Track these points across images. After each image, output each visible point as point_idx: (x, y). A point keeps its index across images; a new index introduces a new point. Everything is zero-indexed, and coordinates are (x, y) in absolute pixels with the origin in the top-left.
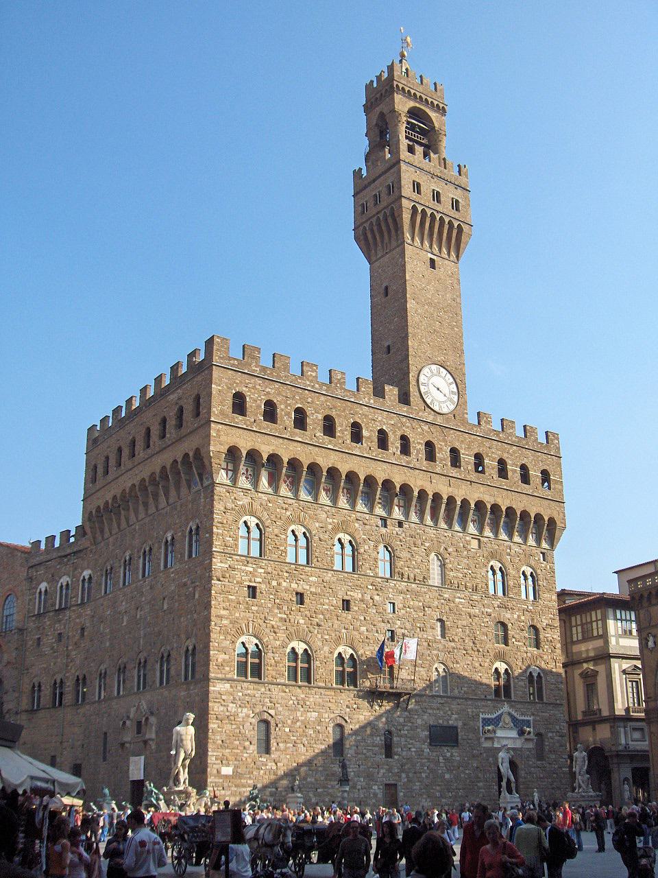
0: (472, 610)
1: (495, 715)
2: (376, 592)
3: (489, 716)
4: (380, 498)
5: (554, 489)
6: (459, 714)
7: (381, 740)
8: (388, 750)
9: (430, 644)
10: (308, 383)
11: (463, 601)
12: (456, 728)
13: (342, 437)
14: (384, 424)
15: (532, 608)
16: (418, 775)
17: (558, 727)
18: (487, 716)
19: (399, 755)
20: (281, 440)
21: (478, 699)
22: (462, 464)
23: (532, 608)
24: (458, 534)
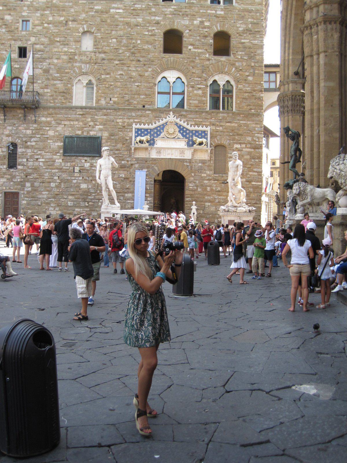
0: (133, 20)
1: (154, 126)
3: (146, 127)
6: (105, 125)
7: (3, 152)
8: (12, 160)
9: (71, 56)
11: (121, 11)
12: (98, 138)
15: (222, 13)
16: (47, 185)
17: (249, 139)
18: (142, 126)
19: (23, 165)
21: (133, 110)
23: (222, 13)
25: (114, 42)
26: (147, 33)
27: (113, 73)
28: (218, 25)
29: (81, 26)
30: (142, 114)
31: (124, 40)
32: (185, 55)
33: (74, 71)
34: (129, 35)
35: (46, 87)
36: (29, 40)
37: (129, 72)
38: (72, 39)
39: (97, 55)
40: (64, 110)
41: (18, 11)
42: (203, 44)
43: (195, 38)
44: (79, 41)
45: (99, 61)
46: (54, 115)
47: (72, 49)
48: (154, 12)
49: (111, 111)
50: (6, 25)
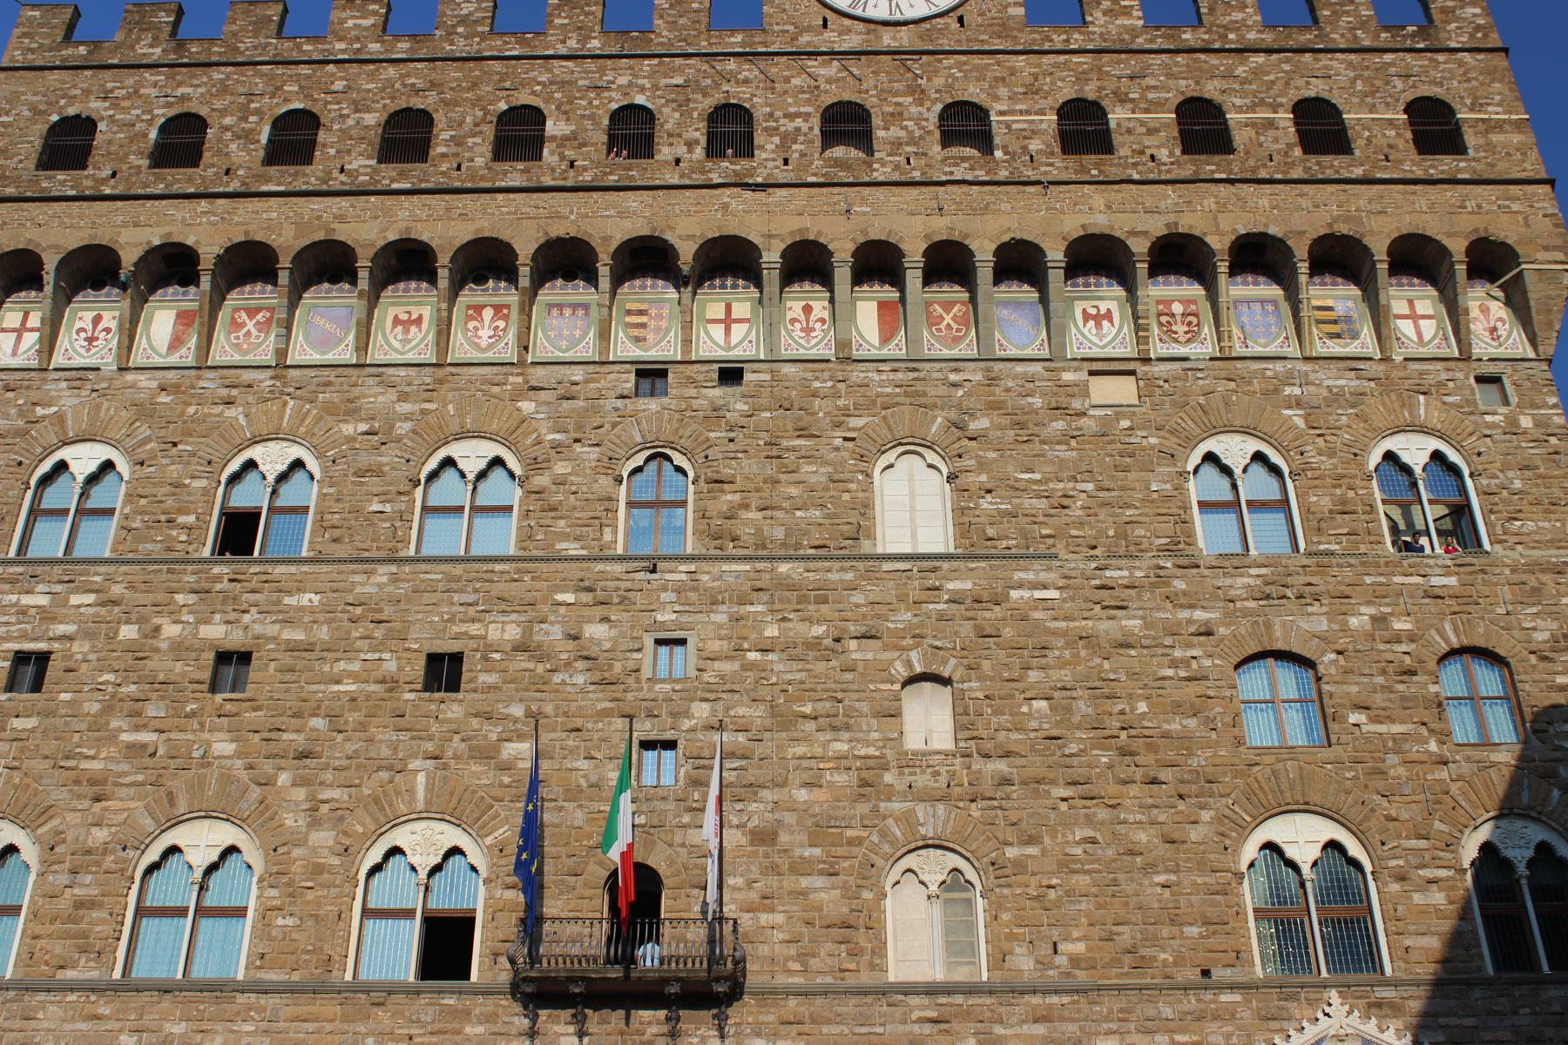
0: (1104, 625)
2: (600, 611)
4: (641, 313)
5: (1490, 147)
9: (865, 774)
10: (340, 46)
13: (457, 154)
14: (642, 89)
15: (1452, 581)
20: (204, 204)
22: (997, 140)
23: (1452, 581)
24: (1020, 368)
25: (1038, 711)
26: (1170, 672)
27: (1054, 837)
28: (1448, 626)
29: (897, 654)
30: (1202, 1006)
31: (1081, 703)
32: (1339, 749)
33: (884, 834)
34: (1098, 684)
35: (767, 901)
36: (687, 714)
37: (1122, 829)
38: (865, 707)
39: (975, 767)
40: (853, 1001)
41: (638, 607)
42: (1407, 702)
43: (1366, 680)
44: (896, 714)
45: (987, 787)
46: (806, 1028)
47: (868, 744)
48: (1185, 594)
49: (1066, 999)
50: (587, 658)
